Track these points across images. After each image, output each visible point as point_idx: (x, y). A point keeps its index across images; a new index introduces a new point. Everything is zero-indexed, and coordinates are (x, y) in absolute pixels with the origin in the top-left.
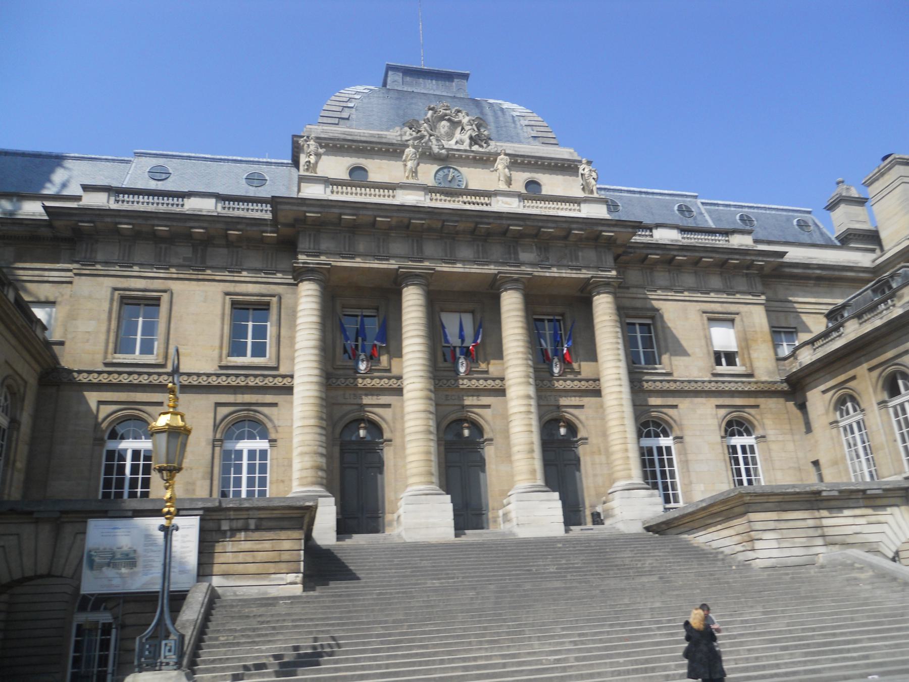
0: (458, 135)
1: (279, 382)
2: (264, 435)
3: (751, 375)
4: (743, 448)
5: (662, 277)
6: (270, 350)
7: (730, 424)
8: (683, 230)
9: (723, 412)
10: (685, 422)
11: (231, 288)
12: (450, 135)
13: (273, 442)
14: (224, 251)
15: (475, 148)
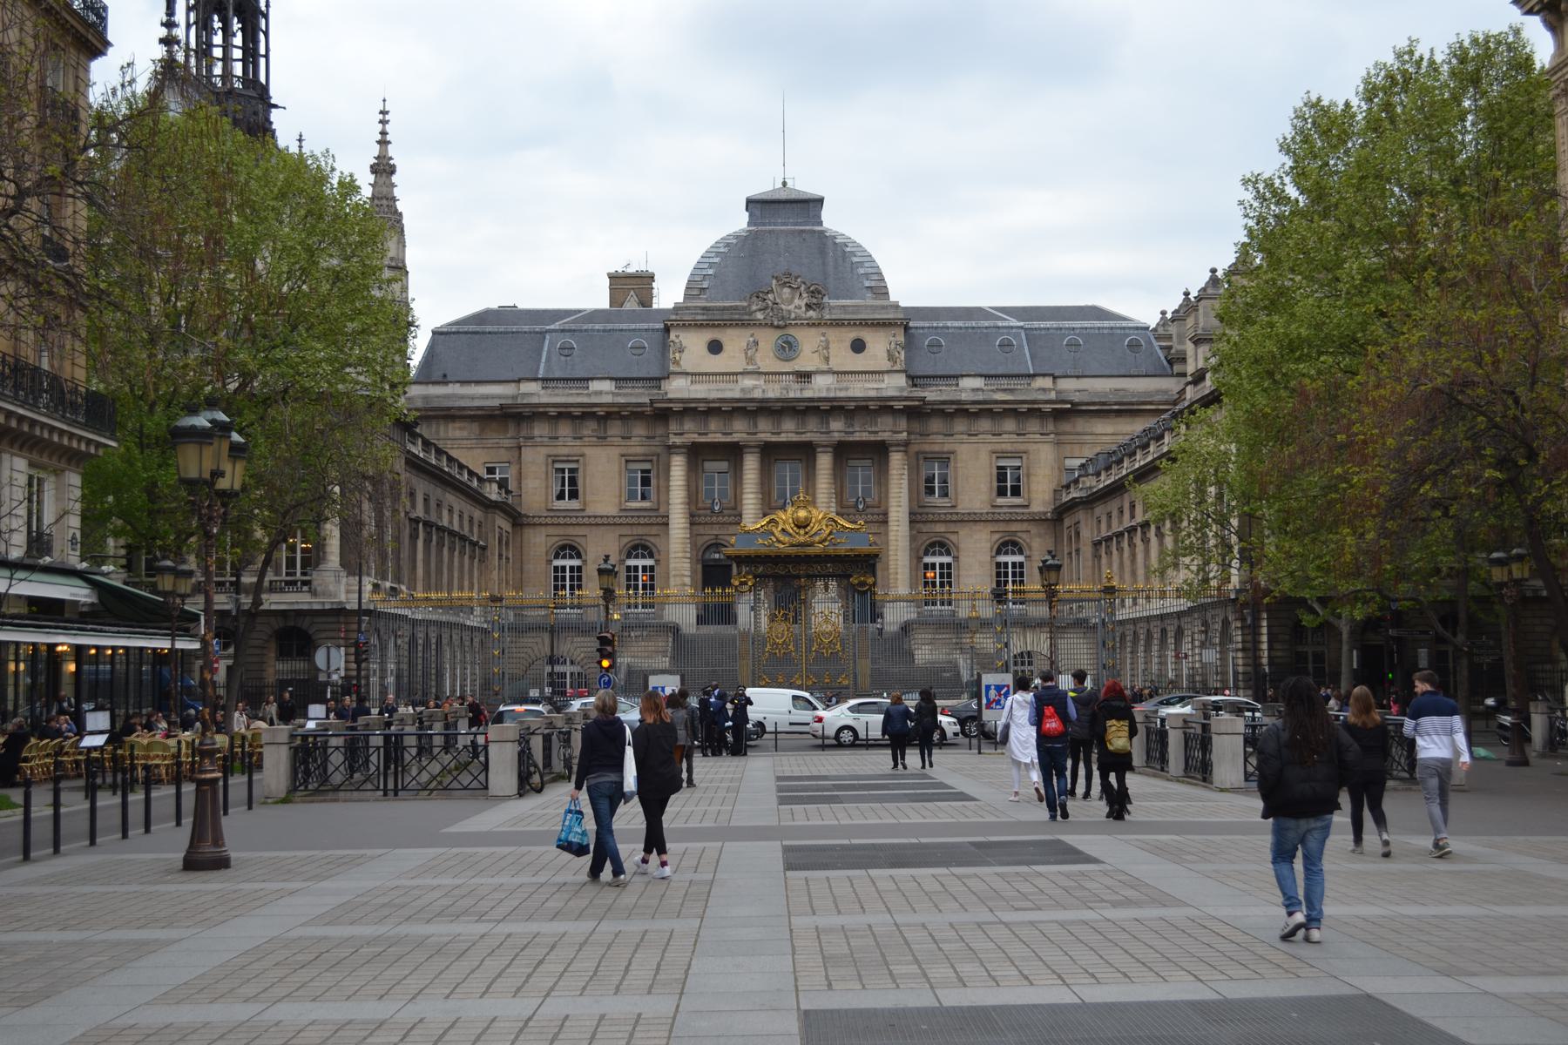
0: (797, 302)
1: (659, 520)
2: (651, 556)
3: (1027, 506)
4: (1014, 564)
5: (960, 425)
6: (653, 496)
7: (1005, 544)
8: (986, 376)
9: (997, 536)
10: (962, 546)
11: (624, 451)
12: (791, 301)
13: (657, 561)
14: (619, 423)
15: (811, 313)
